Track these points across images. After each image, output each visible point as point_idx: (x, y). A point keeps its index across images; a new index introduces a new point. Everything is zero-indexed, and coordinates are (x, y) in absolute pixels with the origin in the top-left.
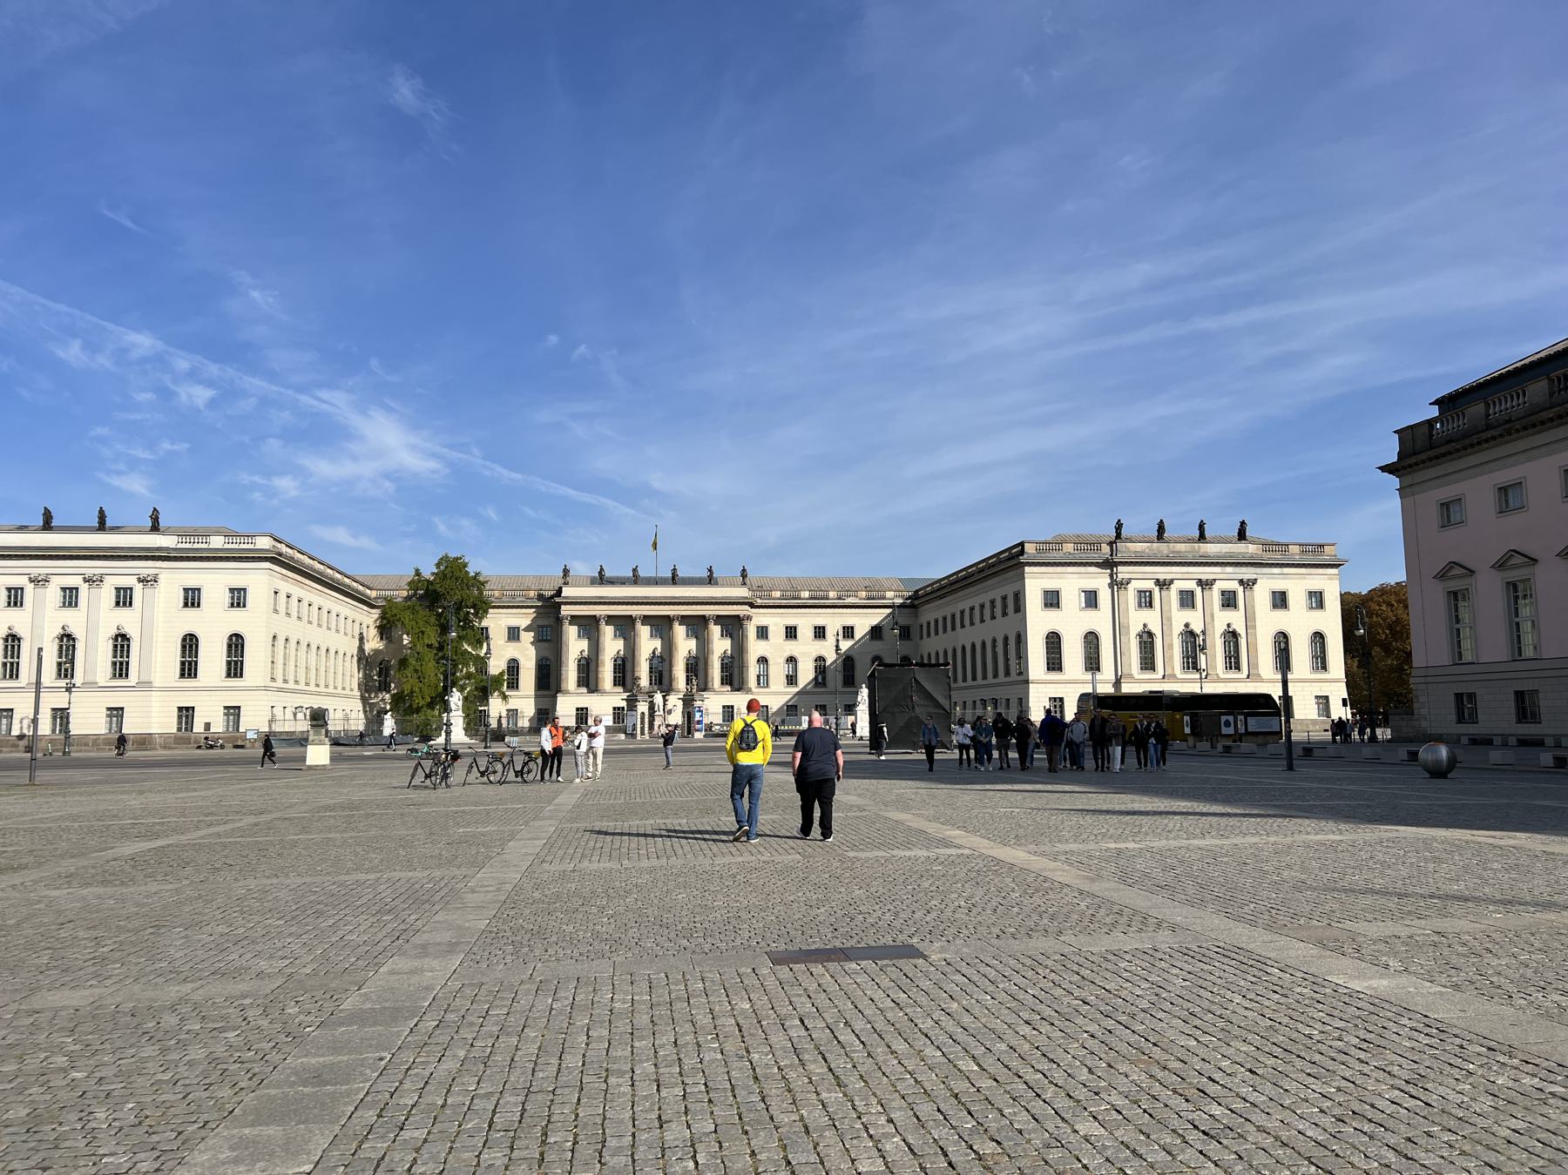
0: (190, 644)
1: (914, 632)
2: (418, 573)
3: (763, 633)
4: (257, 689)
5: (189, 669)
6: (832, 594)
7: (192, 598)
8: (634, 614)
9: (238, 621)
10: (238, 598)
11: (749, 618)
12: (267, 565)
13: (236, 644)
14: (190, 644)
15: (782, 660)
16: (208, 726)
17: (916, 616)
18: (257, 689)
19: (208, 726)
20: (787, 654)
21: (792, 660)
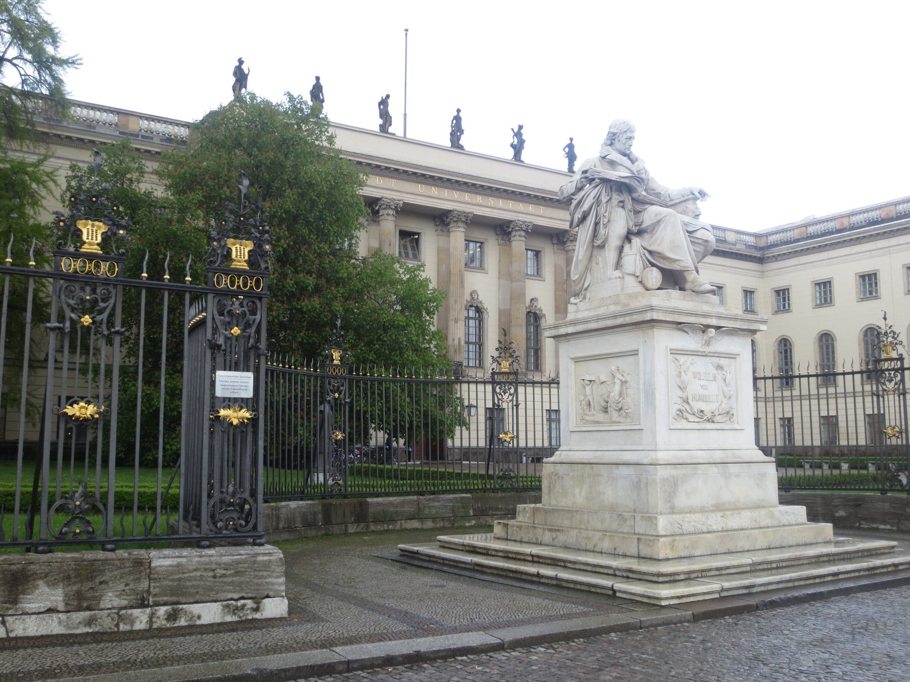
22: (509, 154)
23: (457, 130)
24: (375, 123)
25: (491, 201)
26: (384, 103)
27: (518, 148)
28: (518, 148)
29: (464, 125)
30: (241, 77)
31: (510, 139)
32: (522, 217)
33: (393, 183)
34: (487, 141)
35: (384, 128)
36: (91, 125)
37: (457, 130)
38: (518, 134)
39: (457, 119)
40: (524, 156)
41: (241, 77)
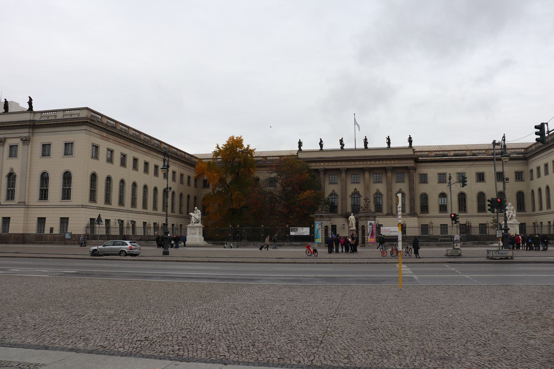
0: (45, 178)
1: (526, 176)
2: (218, 147)
3: (424, 179)
4: (78, 206)
5: (44, 195)
6: (468, 153)
7: (46, 150)
8: (341, 167)
9: (68, 164)
10: (68, 148)
11: (414, 169)
12: (84, 127)
13: (67, 177)
14: (45, 178)
15: (436, 196)
16: (52, 229)
17: (527, 164)
18: (78, 206)
19: (52, 229)
20: (440, 192)
21: (443, 195)
22: (386, 146)
23: (366, 143)
24: (339, 147)
25: (377, 162)
26: (341, 141)
27: (389, 143)
28: (389, 143)
29: (368, 141)
30: (300, 144)
31: (386, 141)
32: (389, 165)
33: (344, 163)
34: (377, 142)
35: (342, 148)
36: (272, 160)
37: (366, 143)
38: (388, 139)
39: (366, 139)
40: (391, 146)
41: (300, 144)
